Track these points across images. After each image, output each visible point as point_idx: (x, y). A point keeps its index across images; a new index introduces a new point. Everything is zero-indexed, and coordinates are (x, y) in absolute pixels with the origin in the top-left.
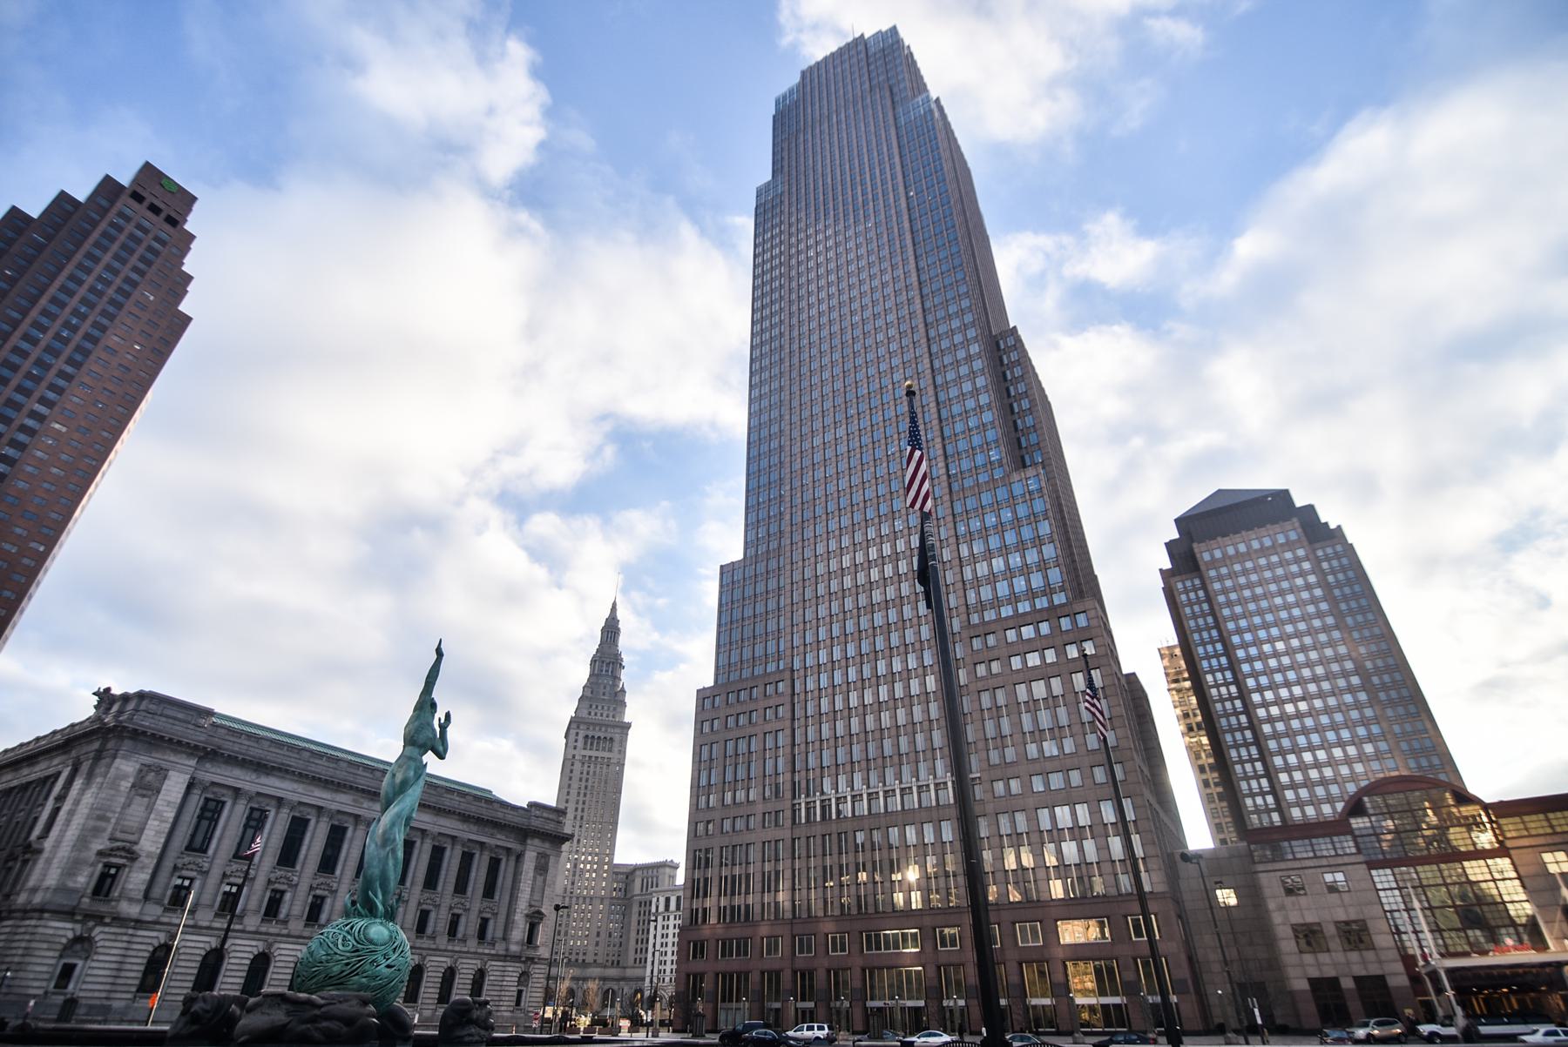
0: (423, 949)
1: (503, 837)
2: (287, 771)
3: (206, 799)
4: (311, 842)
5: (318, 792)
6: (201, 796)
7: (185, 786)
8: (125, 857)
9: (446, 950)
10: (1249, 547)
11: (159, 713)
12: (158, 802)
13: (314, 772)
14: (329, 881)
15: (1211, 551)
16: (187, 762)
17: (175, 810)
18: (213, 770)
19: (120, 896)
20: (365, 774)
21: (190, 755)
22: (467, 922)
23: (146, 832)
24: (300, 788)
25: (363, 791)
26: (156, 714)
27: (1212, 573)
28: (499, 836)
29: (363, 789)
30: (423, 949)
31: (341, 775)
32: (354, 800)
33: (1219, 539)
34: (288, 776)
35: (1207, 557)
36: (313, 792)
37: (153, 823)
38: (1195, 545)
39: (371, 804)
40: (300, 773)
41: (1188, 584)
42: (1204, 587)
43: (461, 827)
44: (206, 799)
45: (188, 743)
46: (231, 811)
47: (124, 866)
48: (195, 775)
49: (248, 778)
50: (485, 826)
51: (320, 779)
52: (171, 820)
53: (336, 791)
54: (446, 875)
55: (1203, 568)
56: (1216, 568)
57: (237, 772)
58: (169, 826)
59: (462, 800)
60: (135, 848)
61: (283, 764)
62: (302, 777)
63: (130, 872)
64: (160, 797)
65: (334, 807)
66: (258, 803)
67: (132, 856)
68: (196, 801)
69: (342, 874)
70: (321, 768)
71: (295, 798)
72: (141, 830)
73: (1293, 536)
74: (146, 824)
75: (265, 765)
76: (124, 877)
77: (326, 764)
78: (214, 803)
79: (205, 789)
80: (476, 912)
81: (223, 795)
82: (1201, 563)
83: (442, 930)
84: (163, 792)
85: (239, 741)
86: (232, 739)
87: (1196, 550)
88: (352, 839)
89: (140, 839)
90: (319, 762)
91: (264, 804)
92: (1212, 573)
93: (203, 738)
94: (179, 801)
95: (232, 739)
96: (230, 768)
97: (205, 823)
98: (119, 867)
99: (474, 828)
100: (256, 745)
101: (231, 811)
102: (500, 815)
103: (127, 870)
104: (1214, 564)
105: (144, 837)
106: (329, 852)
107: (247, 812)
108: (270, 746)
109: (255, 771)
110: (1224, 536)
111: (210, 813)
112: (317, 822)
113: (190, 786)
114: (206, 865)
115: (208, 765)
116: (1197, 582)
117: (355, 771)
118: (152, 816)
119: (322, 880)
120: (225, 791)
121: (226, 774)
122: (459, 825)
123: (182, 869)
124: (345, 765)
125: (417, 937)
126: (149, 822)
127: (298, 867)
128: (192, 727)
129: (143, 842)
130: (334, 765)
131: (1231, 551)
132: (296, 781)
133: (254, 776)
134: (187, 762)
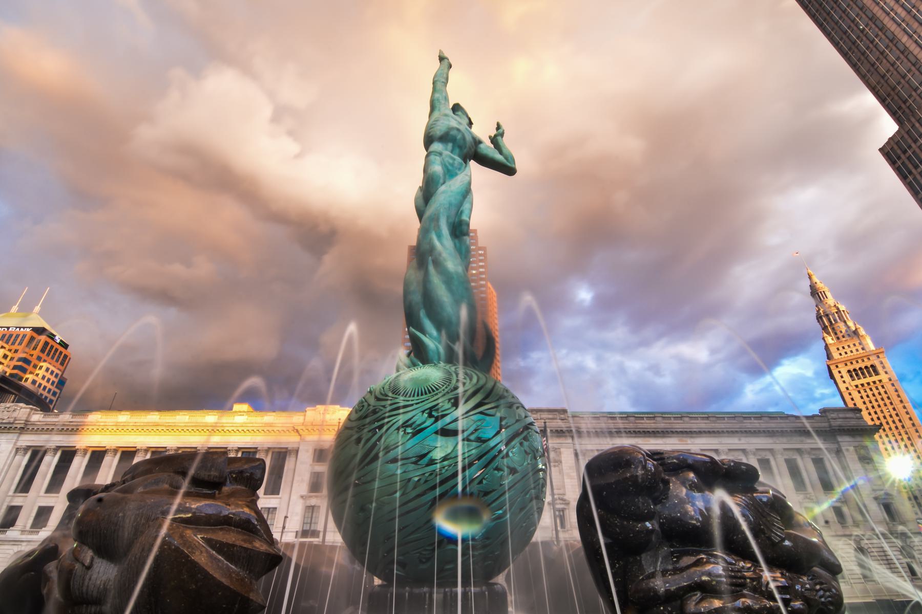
7: (573, 456)
8: (563, 504)
11: (539, 418)
12: (564, 468)
13: (643, 428)
16: (567, 442)
17: (575, 471)
19: (571, 527)
23: (566, 487)
26: (538, 419)
29: (681, 431)
32: (679, 440)
37: (567, 481)
39: (692, 440)
40: (634, 431)
47: (565, 508)
48: (575, 448)
49: (605, 443)
51: (648, 431)
52: (576, 477)
53: (664, 437)
58: (576, 480)
60: (565, 497)
63: (569, 512)
64: (563, 465)
67: (568, 504)
72: (564, 487)
74: (564, 482)
76: (568, 515)
79: (584, 455)
84: (563, 462)
89: (565, 491)
94: (574, 465)
98: (563, 510)
103: (567, 511)
105: (567, 490)
108: (607, 420)
113: (576, 455)
117: (670, 421)
118: (565, 477)
124: (660, 419)
126: (566, 480)
128: (560, 421)
129: (567, 493)
130: (654, 421)
132: (635, 437)
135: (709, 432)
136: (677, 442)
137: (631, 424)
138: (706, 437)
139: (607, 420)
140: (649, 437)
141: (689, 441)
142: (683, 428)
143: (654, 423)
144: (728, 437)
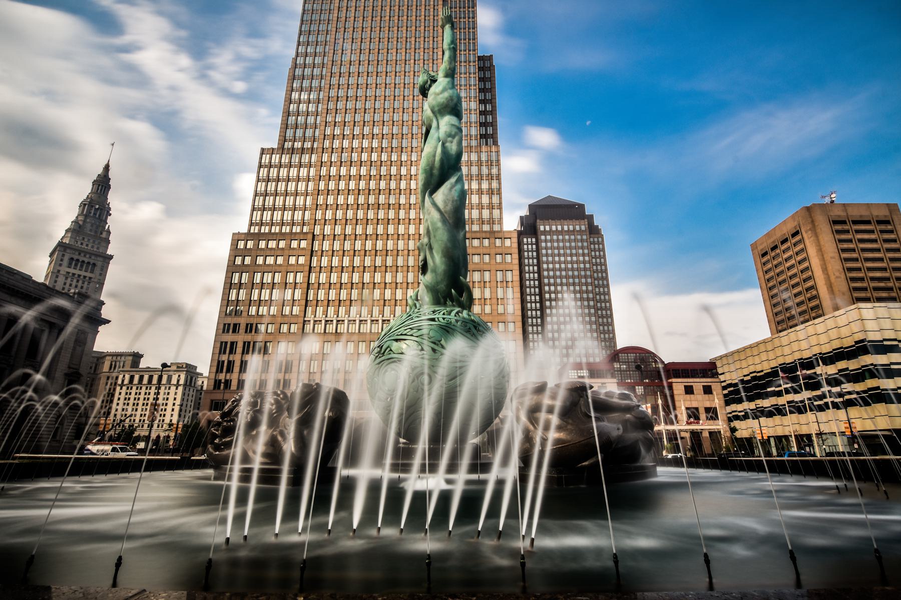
10: (563, 228)
15: (544, 226)
27: (543, 237)
33: (550, 220)
35: (542, 228)
38: (538, 221)
41: (529, 240)
42: (537, 244)
55: (539, 233)
56: (545, 236)
73: (583, 228)
82: (539, 231)
87: (538, 224)
92: (543, 237)
104: (545, 233)
110: (552, 220)
116: (534, 240)
131: (554, 228)
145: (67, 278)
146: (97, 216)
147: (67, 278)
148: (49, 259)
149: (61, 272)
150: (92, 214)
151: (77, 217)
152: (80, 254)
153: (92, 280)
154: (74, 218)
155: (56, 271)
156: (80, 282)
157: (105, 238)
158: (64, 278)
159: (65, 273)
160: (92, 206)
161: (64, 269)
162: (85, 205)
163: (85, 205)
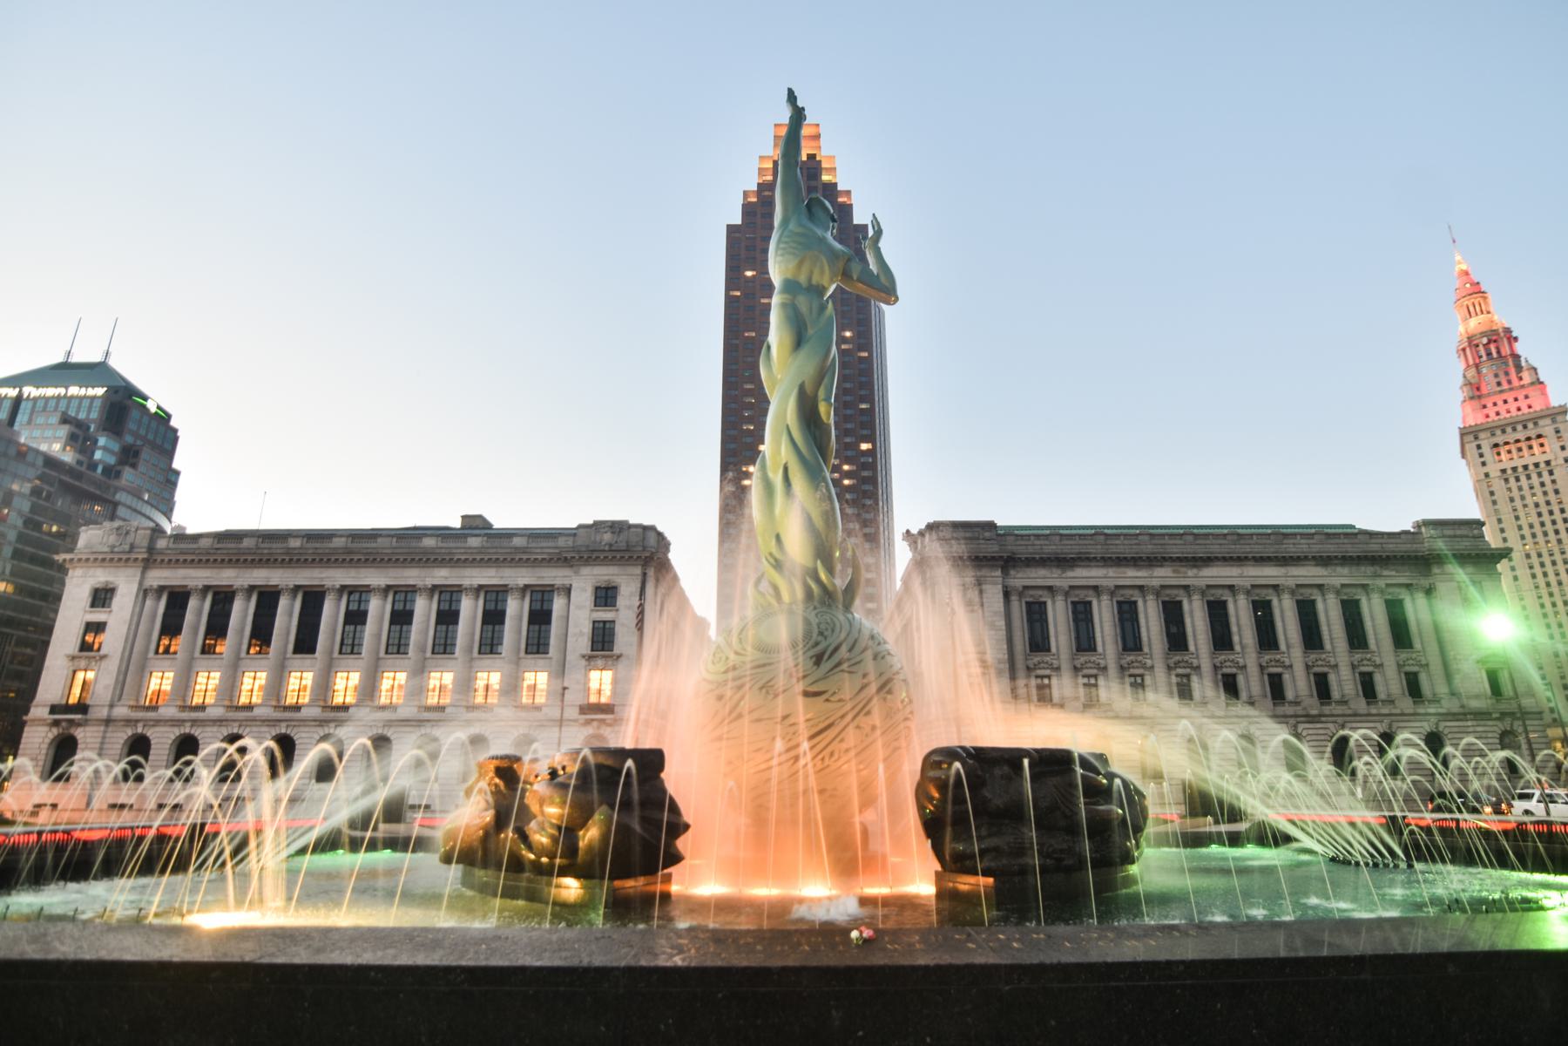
0: (1338, 716)
1: (1393, 573)
2: (1088, 559)
3: (1027, 603)
4: (1147, 622)
5: (1131, 572)
6: (1020, 601)
9: (1369, 715)
14: (1186, 658)
16: (993, 574)
17: (1003, 618)
18: (1019, 575)
20: (1171, 542)
21: (993, 567)
22: (1386, 680)
24: (1111, 572)
25: (1179, 559)
28: (1386, 573)
29: (1178, 558)
30: (1338, 716)
31: (1148, 549)
32: (1174, 571)
34: (1093, 564)
36: (1125, 573)
43: (1325, 573)
44: (1027, 603)
45: (985, 557)
46: (1054, 610)
50: (1358, 565)
51: (1125, 558)
54: (1330, 631)
57: (1042, 572)
59: (1312, 541)
61: (1080, 553)
62: (1107, 561)
65: (1156, 583)
66: (1077, 596)
68: (1018, 609)
69: (1197, 649)
70: (1122, 548)
71: (1111, 583)
75: (1065, 558)
77: (1126, 542)
78: (1037, 606)
80: (1394, 667)
81: (1041, 596)
83: (1353, 692)
85: (1030, 543)
86: (1023, 543)
88: (1191, 612)
90: (1117, 542)
91: (1082, 595)
93: (996, 548)
95: (1023, 543)
96: (1034, 570)
97: (1038, 625)
99: (1345, 570)
100: (1047, 542)
101: (1054, 610)
102: (1374, 547)
106: (1174, 630)
107: (1070, 606)
108: (1061, 540)
109: (1058, 566)
111: (1036, 615)
112: (1145, 601)
114: (1054, 662)
115: (1012, 572)
119: (1178, 658)
120: (1040, 592)
121: (1032, 576)
122: (1320, 571)
123: (1035, 669)
124: (1147, 538)
125: (1322, 704)
127: (1146, 649)
132: (1103, 566)
133: (1059, 572)
134: (993, 574)
135: (1224, 559)
136: (1172, 575)
137: (1099, 547)
138: (1217, 566)
139: (1061, 540)
140: (1127, 566)
141: (1191, 573)
142: (1183, 553)
143: (1136, 544)
144: (1254, 566)
145: (1506, 480)
146: (1495, 355)
147: (1506, 480)
148: (1464, 461)
149: (1492, 475)
150: (1484, 358)
151: (1465, 376)
152: (1504, 432)
153: (1553, 463)
154: (1460, 380)
155: (1483, 477)
156: (1523, 478)
157: (1532, 384)
158: (1503, 482)
159: (1499, 474)
160: (1477, 346)
161: (1494, 469)
162: (1464, 350)
163: (1464, 350)
